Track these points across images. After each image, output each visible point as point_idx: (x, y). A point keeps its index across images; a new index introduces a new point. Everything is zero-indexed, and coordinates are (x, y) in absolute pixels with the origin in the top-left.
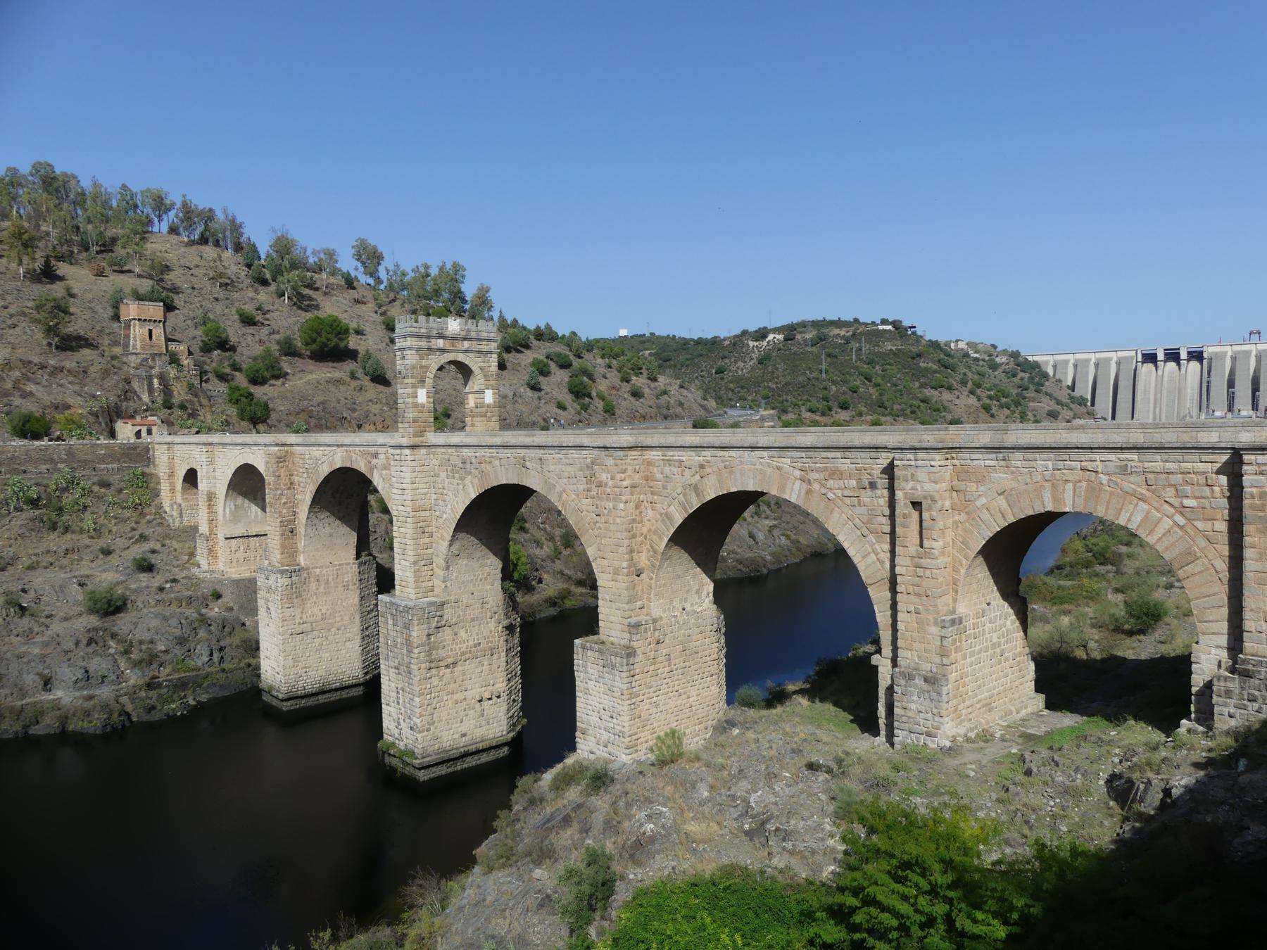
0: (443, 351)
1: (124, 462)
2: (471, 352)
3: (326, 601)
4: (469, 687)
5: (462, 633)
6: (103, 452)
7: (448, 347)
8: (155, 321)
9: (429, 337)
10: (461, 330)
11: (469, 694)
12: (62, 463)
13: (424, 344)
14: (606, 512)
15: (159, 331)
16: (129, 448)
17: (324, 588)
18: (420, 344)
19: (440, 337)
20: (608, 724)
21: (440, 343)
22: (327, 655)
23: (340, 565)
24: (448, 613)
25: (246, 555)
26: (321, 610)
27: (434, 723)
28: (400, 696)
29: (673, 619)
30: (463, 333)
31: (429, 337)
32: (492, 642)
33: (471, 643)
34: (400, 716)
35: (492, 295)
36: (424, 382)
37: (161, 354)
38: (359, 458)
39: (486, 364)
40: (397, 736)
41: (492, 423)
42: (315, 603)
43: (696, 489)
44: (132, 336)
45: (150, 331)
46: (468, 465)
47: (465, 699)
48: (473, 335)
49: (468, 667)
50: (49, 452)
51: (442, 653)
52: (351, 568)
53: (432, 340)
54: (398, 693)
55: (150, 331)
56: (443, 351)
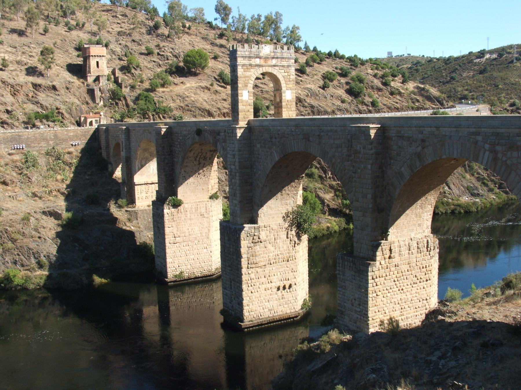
0: (259, 66)
1: (83, 140)
5: (270, 246)
6: (72, 134)
8: (100, 56)
9: (250, 57)
11: (273, 284)
12: (52, 141)
13: (246, 62)
14: (359, 170)
16: (85, 132)
19: (257, 57)
20: (357, 309)
21: (258, 61)
22: (193, 256)
25: (147, 195)
28: (232, 284)
30: (272, 54)
31: (250, 57)
34: (233, 296)
35: (300, 33)
36: (247, 86)
37: (102, 76)
38: (209, 136)
39: (286, 74)
40: (230, 308)
42: (185, 225)
43: (419, 156)
44: (88, 66)
45: (97, 63)
46: (274, 140)
48: (279, 55)
49: (274, 267)
50: (45, 134)
51: (258, 259)
52: (206, 204)
53: (252, 59)
54: (231, 282)
55: (97, 63)
56: (259, 66)
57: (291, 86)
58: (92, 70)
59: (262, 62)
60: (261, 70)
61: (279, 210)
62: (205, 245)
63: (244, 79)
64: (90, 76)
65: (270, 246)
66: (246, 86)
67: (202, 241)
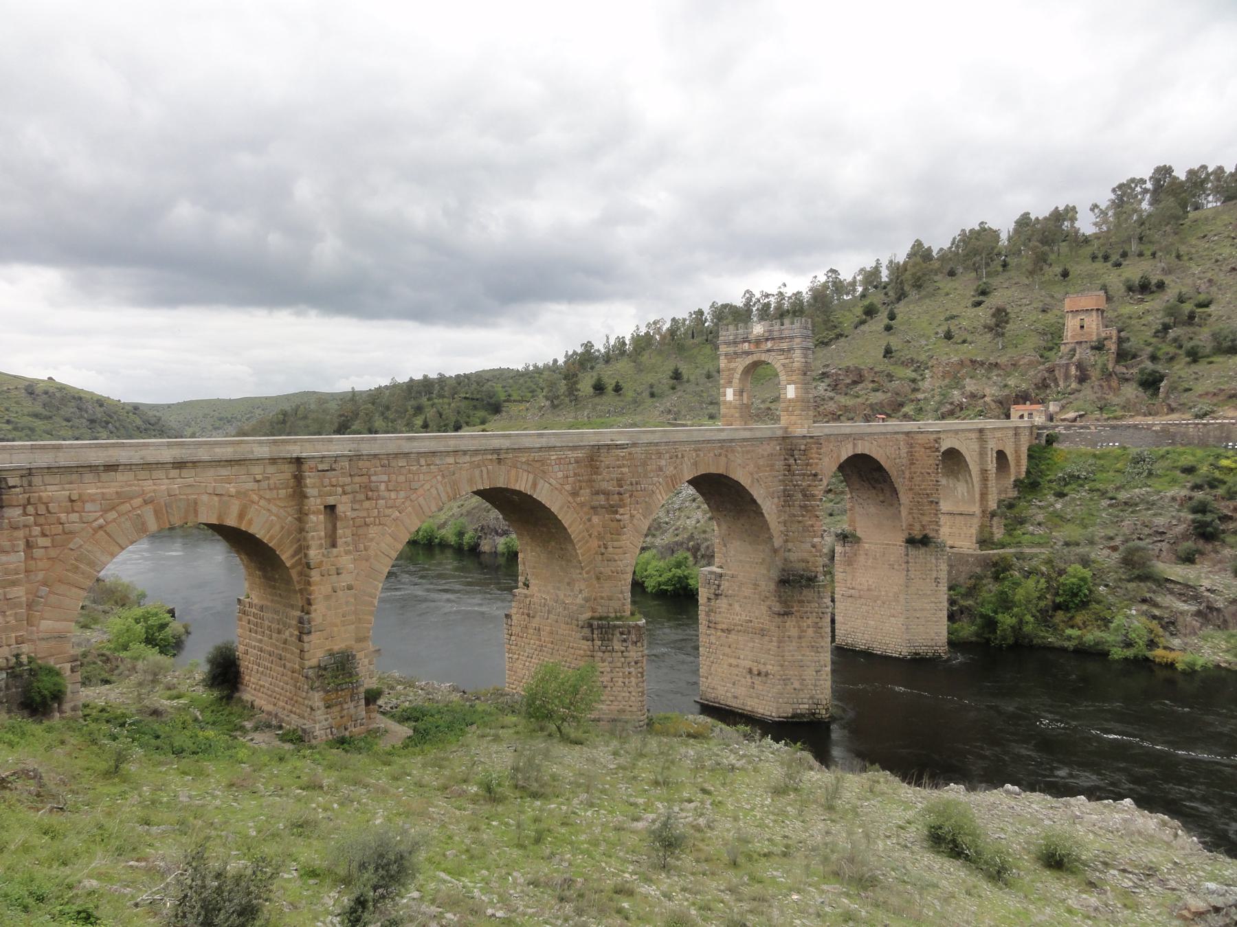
0: (748, 353)
2: (773, 350)
4: (742, 657)
5: (737, 607)
7: (753, 348)
13: (731, 349)
19: (744, 342)
24: (725, 585)
30: (766, 334)
31: (735, 343)
32: (763, 624)
39: (787, 361)
47: (737, 666)
48: (776, 334)
56: (748, 353)
57: (794, 378)
58: (1069, 334)
60: (749, 360)
63: (727, 373)
65: (737, 607)
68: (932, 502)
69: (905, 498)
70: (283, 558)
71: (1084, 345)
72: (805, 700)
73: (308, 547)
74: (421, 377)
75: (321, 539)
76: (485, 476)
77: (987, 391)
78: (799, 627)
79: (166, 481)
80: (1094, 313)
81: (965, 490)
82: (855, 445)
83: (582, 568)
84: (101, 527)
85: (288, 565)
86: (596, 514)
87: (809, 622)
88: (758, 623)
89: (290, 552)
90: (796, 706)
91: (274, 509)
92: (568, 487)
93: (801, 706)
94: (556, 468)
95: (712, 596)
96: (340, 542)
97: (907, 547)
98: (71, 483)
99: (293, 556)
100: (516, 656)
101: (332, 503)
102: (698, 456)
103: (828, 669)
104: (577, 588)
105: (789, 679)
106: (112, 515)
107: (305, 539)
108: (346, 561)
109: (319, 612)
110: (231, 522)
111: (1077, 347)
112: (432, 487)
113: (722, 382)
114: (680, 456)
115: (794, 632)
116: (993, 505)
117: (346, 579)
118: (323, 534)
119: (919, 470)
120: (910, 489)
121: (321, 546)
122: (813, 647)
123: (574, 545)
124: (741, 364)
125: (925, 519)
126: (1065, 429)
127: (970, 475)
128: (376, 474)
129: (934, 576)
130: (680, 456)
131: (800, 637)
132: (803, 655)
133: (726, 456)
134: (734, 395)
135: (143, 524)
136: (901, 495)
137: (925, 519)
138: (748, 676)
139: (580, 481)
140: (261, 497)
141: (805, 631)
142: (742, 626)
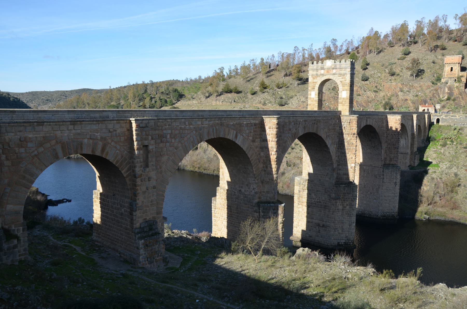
3: (367, 180)
4: (315, 218)
10: (332, 65)
13: (315, 73)
15: (456, 68)
17: (367, 175)
18: (313, 73)
19: (322, 69)
21: (322, 72)
22: (366, 202)
23: (374, 167)
26: (364, 183)
27: (299, 226)
29: (233, 193)
30: (333, 66)
32: (326, 203)
33: (316, 200)
36: (314, 88)
37: (451, 78)
39: (343, 79)
41: (345, 107)
42: (363, 180)
45: (452, 68)
47: (312, 222)
48: (338, 66)
52: (379, 169)
55: (452, 68)
56: (323, 75)
58: (446, 74)
59: (325, 72)
61: (321, 172)
62: (375, 197)
64: (443, 78)
66: (313, 89)
67: (373, 193)
68: (395, 148)
69: (384, 146)
70: (123, 172)
71: (452, 79)
72: (344, 238)
73: (135, 167)
74: (141, 83)
75: (141, 163)
76: (215, 131)
77: (408, 98)
78: (343, 205)
79: (67, 131)
80: (457, 64)
81: (404, 143)
82: (367, 121)
83: (255, 178)
84: (36, 155)
85: (125, 176)
86: (262, 151)
87: (348, 203)
88: (324, 203)
89: (126, 169)
90: (339, 241)
91: (118, 147)
92: (251, 138)
93: (342, 241)
94: (246, 128)
95: (301, 190)
96: (150, 164)
97: (383, 168)
98: (20, 131)
99: (127, 171)
100: (218, 219)
101: (147, 144)
102: (305, 124)
103: (354, 224)
104: (252, 187)
105: (337, 229)
106: (41, 149)
107: (133, 162)
108: (153, 174)
109: (140, 199)
110: (98, 153)
111: (449, 80)
112: (191, 136)
113: (309, 88)
114: (298, 123)
115: (340, 207)
116: (415, 149)
117: (153, 183)
118: (142, 160)
119: (391, 133)
120: (386, 142)
121: (141, 166)
122: (348, 214)
123: (252, 167)
124: (319, 81)
125: (392, 156)
126: (445, 116)
127: (408, 136)
128: (165, 129)
129: (394, 182)
130: (298, 123)
131: (343, 210)
132: (344, 218)
133: (317, 124)
134: (316, 95)
135: (57, 154)
136: (383, 145)
137: (392, 156)
138: (317, 228)
139: (256, 135)
140: (112, 141)
141: (346, 207)
142: (315, 204)
